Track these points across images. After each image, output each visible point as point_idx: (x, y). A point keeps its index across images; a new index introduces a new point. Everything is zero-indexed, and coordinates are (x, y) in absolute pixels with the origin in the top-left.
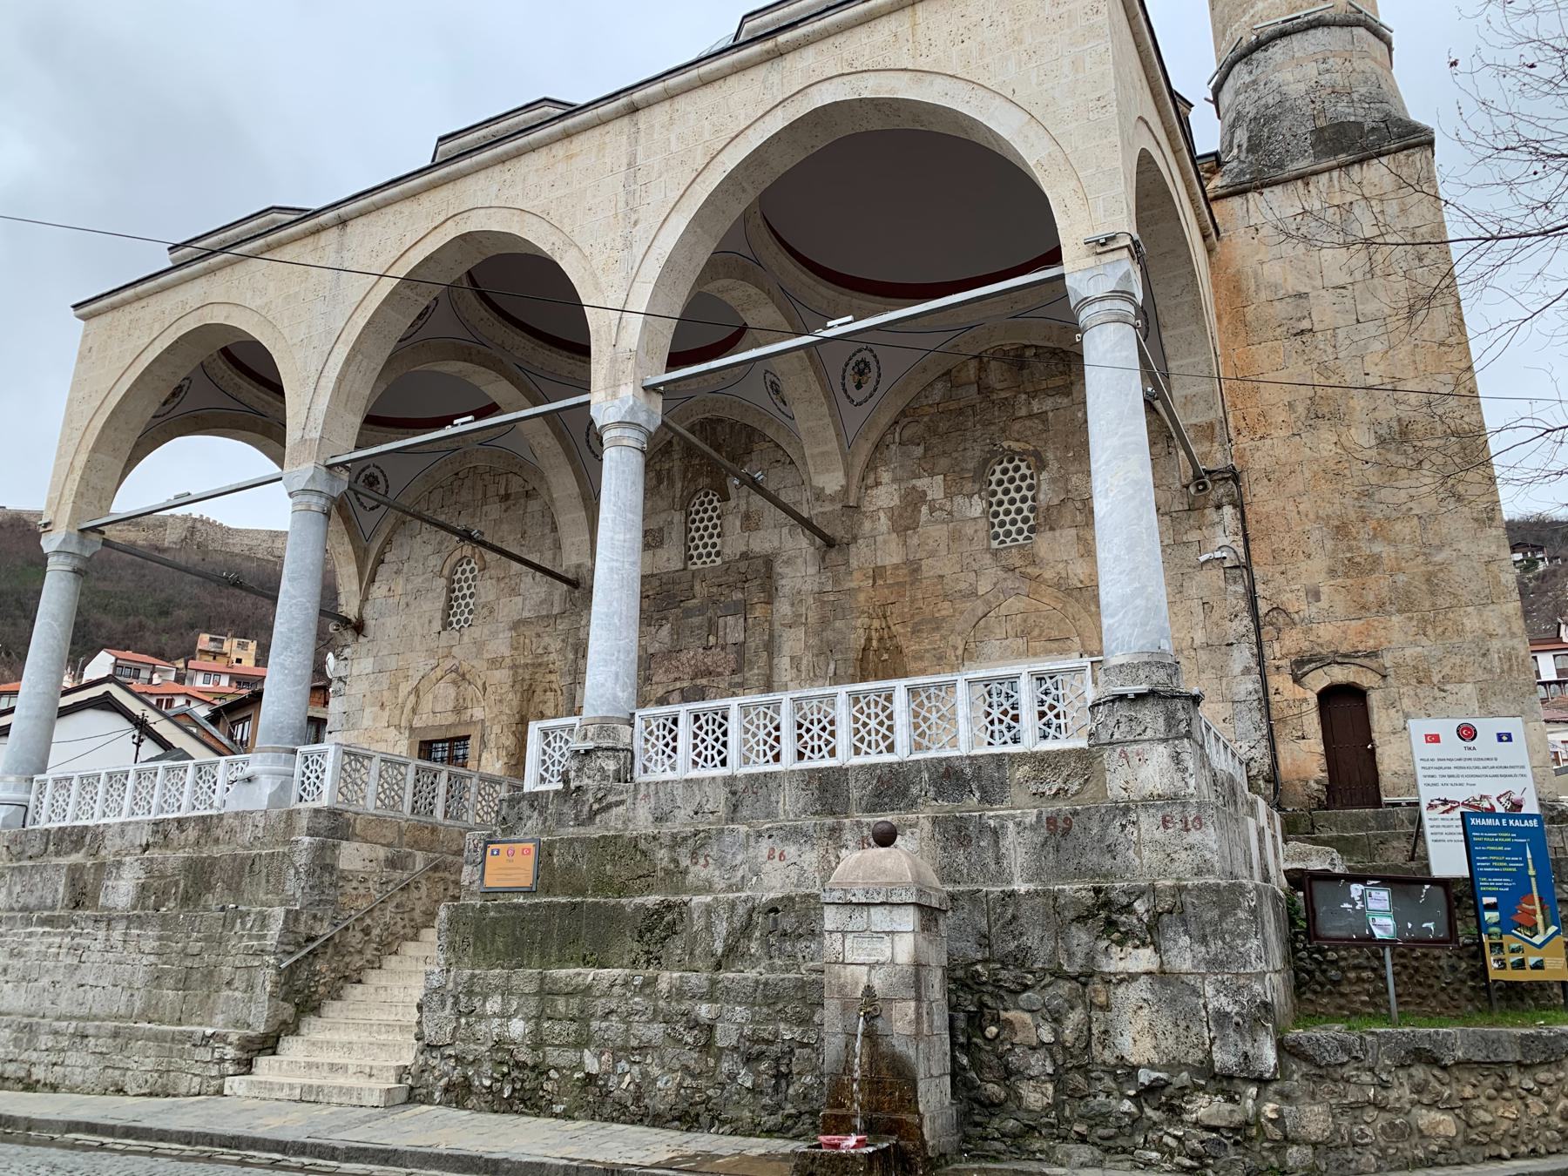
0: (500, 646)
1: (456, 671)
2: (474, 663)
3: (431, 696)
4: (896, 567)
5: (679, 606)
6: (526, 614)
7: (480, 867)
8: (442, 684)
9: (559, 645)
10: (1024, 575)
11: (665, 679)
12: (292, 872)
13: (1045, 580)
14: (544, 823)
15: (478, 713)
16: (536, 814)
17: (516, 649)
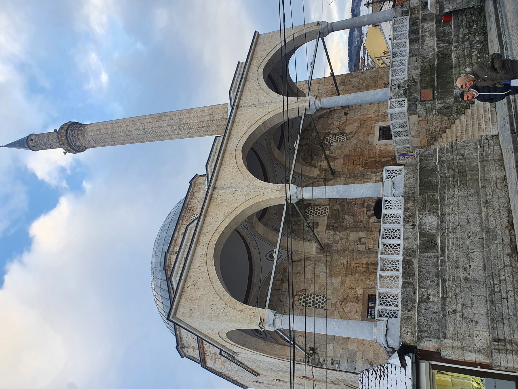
0: (336, 281)
1: (342, 302)
2: (341, 293)
3: (350, 314)
4: (344, 160)
5: (340, 213)
6: (328, 272)
7: (426, 102)
8: (345, 309)
9: (342, 258)
10: (354, 134)
11: (362, 216)
12: (426, 152)
13: (357, 130)
14: (416, 92)
15: (360, 292)
16: (414, 94)
17: (339, 275)
